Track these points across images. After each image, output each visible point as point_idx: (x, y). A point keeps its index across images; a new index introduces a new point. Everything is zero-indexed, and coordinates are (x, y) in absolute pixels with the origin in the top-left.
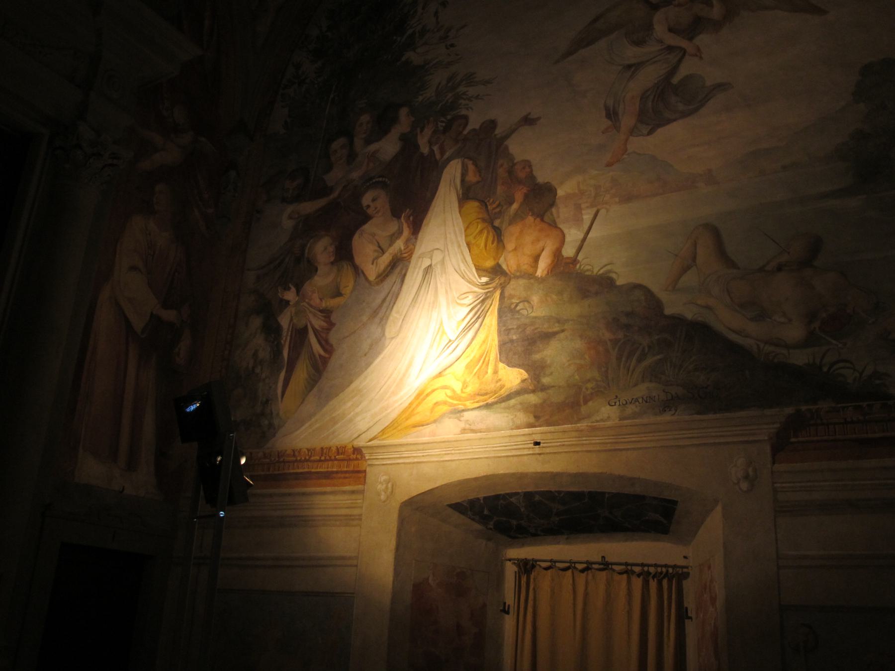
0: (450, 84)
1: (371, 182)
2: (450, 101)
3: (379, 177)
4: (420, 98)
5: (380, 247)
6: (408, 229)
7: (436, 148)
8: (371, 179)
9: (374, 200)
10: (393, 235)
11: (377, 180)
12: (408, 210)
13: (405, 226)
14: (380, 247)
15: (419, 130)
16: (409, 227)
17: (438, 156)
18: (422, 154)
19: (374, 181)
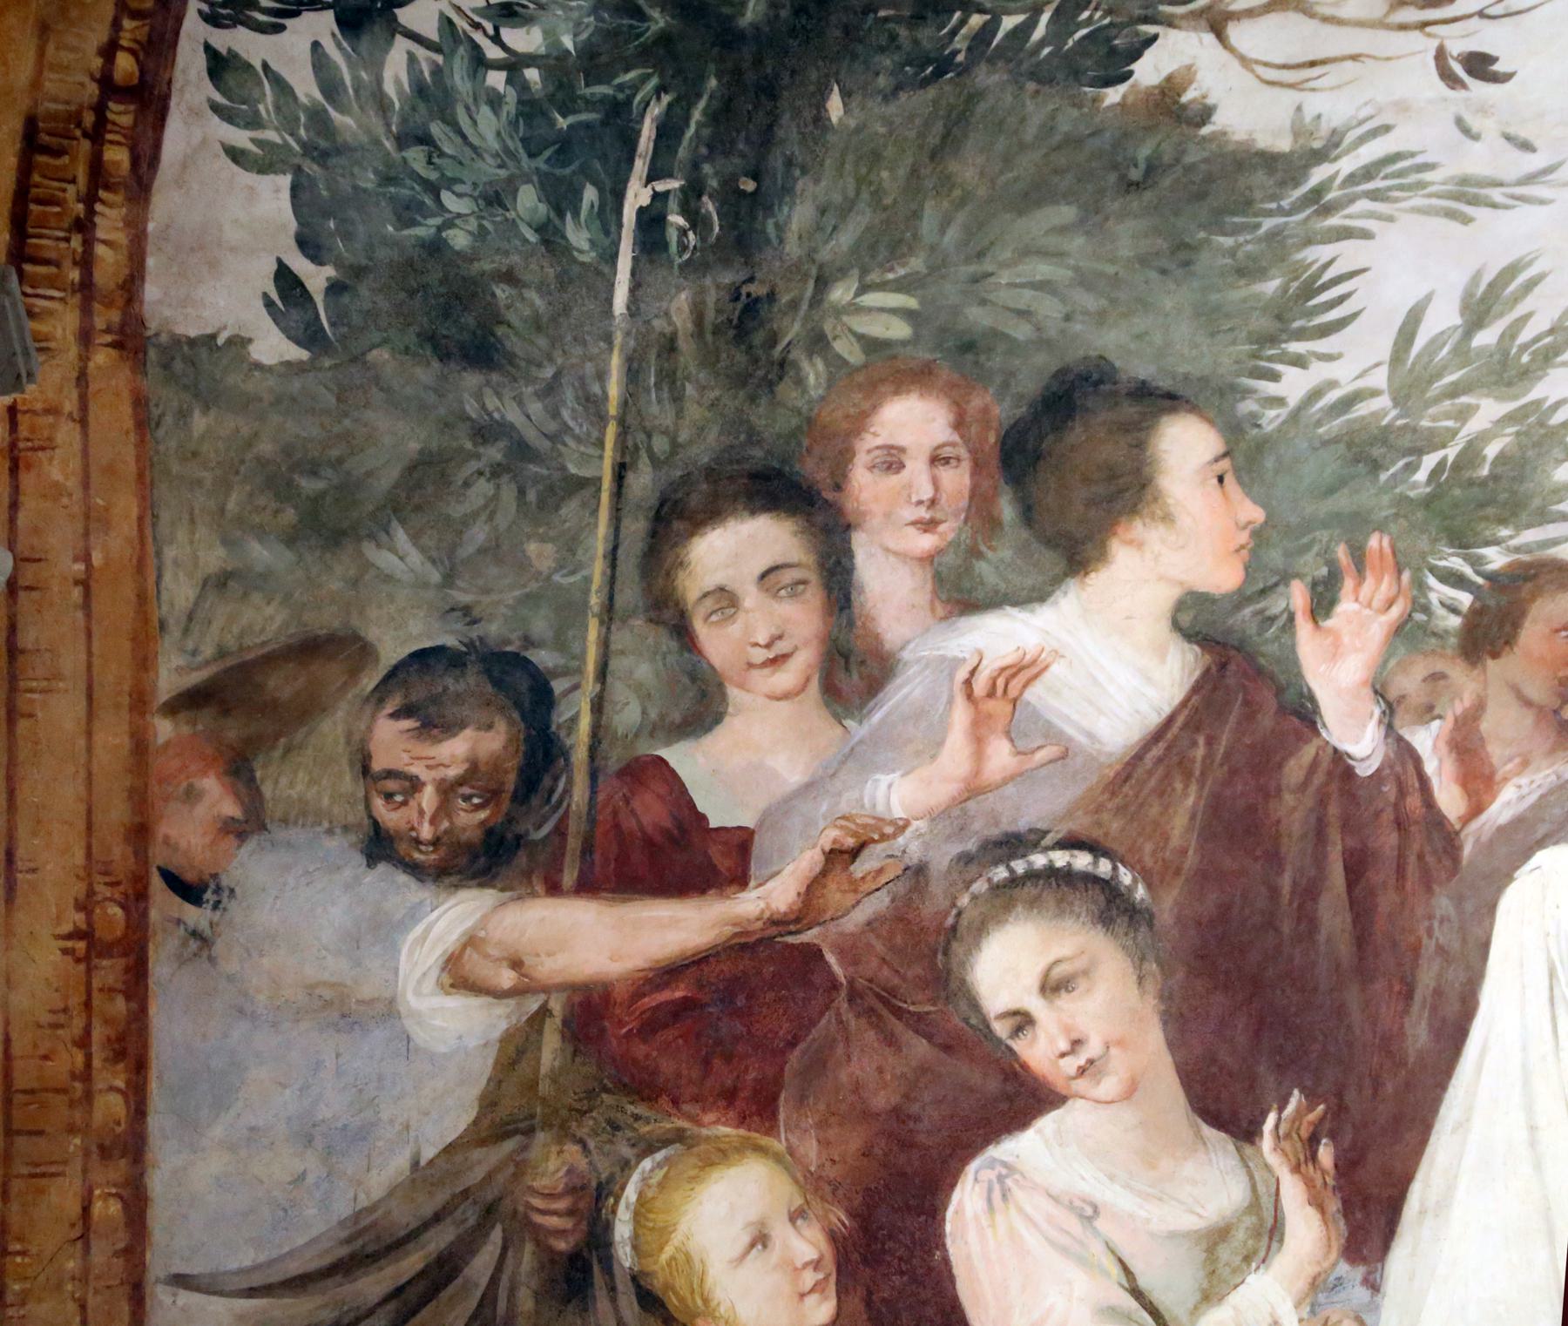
0: (1486, 338)
1: (1019, 866)
2: (1492, 450)
3: (1071, 843)
4: (1293, 384)
5: (1137, 1293)
6: (1312, 1214)
7: (1426, 740)
8: (1013, 844)
9: (1052, 986)
10: (1218, 1235)
11: (1060, 858)
12: (1296, 1099)
13: (1293, 1193)
14: (1137, 1293)
15: (1298, 596)
16: (1317, 1203)
17: (1449, 799)
18: (1340, 764)
19: (1039, 860)
